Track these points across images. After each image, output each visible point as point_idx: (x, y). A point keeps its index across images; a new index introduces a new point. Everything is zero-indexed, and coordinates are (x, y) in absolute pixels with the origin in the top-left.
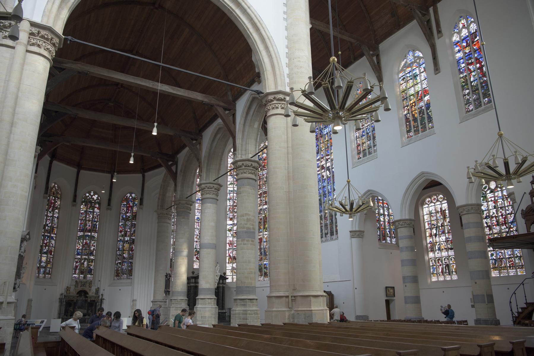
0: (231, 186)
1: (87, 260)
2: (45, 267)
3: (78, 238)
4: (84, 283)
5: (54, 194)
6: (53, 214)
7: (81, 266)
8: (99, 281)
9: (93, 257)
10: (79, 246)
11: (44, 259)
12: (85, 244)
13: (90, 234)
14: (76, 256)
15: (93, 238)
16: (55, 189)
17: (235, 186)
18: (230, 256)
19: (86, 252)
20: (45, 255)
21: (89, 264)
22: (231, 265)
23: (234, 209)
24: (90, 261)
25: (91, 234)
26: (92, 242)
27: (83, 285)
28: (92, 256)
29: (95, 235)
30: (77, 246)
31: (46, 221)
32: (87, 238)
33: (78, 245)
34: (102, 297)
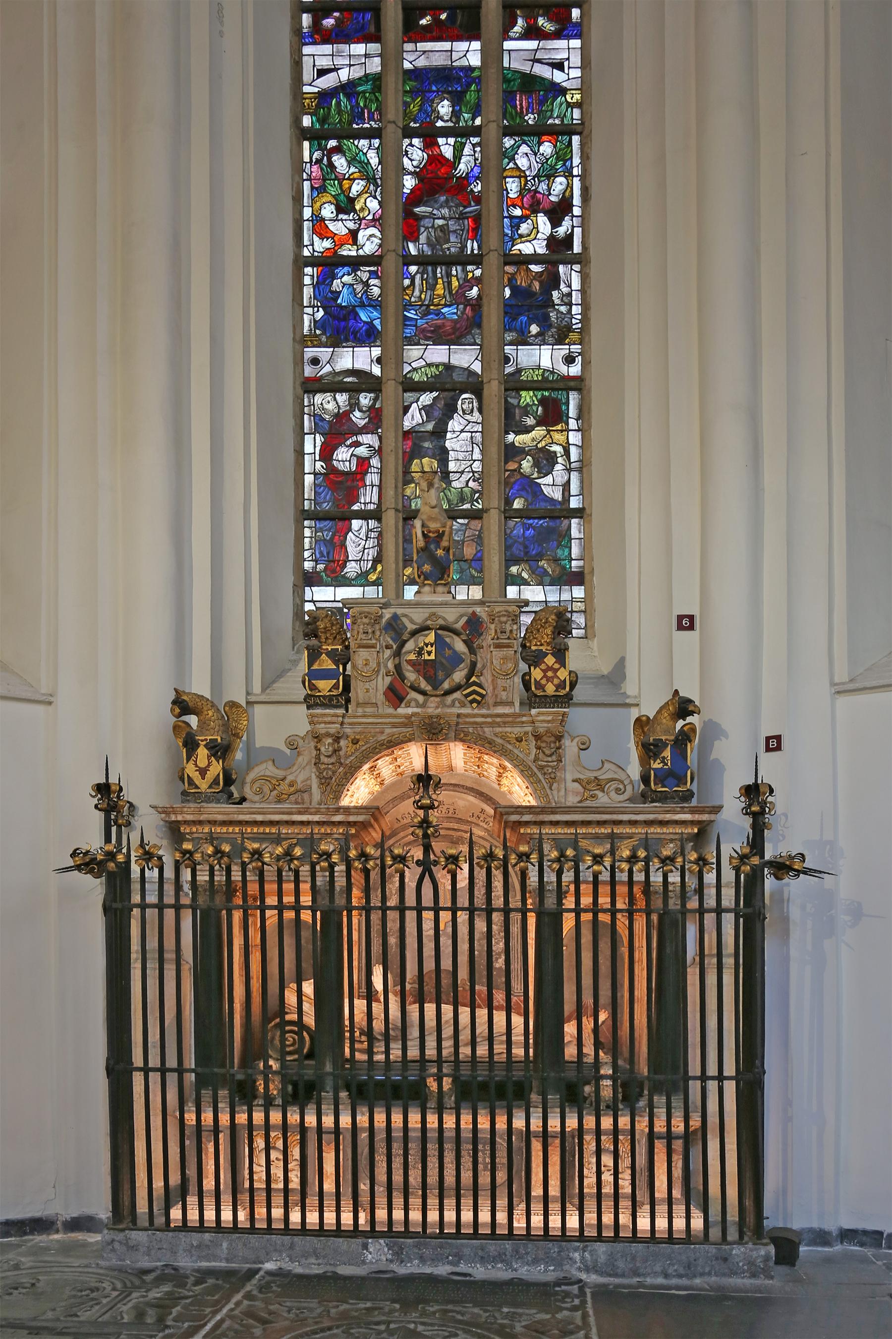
1: (478, 392)
3: (307, 121)
4: (439, 642)
7: (407, 478)
8: (686, 623)
9: (563, 350)
10: (339, 228)
12: (416, 198)
13: (475, 60)
14: (324, 353)
15: (521, 101)
19: (459, 298)
21: (520, 440)
24: (526, 411)
25: (492, 54)
26: (522, 162)
27: (427, 669)
28: (541, 339)
29: (559, 66)
30: (320, 227)
32: (445, 108)
33: (328, 211)
34: (757, 843)
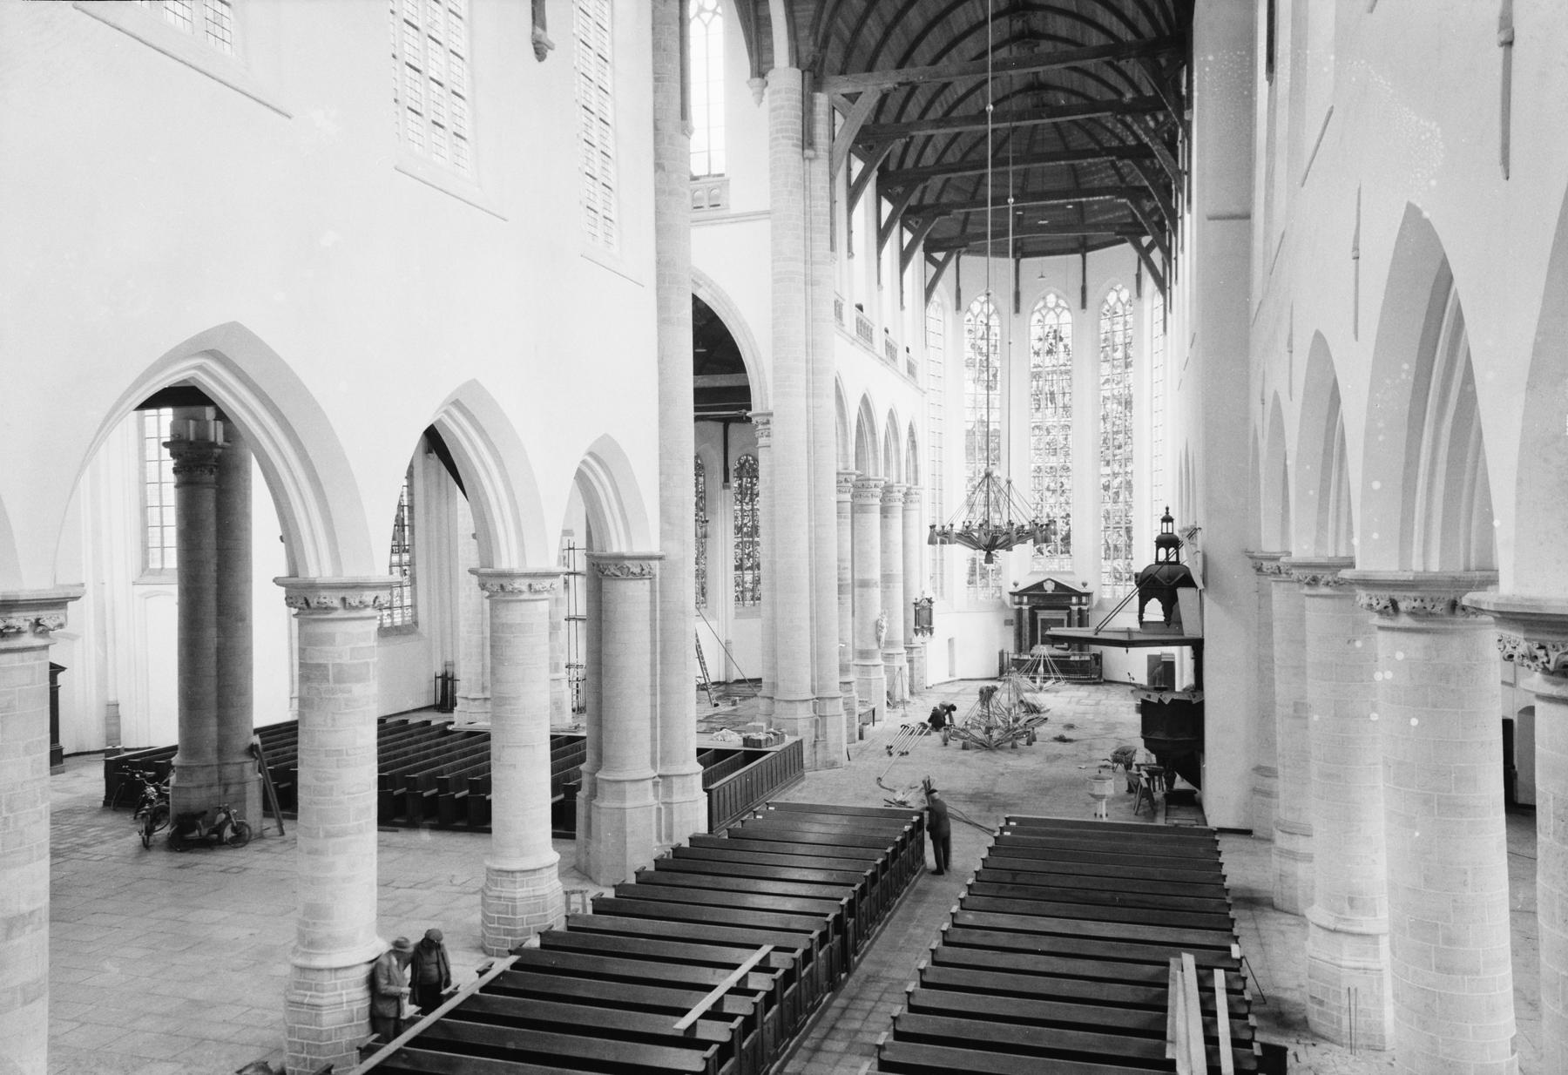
0: (1106, 386)
2: (753, 590)
5: (748, 472)
6: (753, 505)
11: (748, 577)
16: (750, 464)
17: (1114, 386)
18: (1106, 541)
20: (751, 572)
22: (1109, 562)
23: (1114, 439)
31: (743, 519)
